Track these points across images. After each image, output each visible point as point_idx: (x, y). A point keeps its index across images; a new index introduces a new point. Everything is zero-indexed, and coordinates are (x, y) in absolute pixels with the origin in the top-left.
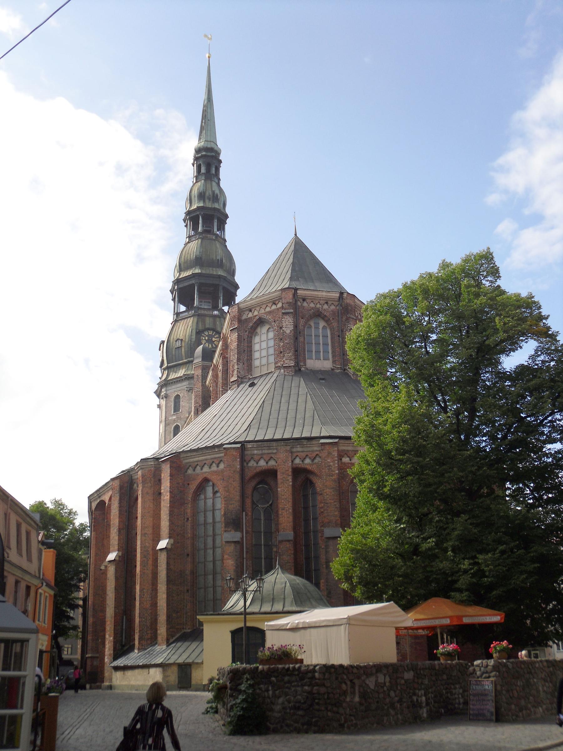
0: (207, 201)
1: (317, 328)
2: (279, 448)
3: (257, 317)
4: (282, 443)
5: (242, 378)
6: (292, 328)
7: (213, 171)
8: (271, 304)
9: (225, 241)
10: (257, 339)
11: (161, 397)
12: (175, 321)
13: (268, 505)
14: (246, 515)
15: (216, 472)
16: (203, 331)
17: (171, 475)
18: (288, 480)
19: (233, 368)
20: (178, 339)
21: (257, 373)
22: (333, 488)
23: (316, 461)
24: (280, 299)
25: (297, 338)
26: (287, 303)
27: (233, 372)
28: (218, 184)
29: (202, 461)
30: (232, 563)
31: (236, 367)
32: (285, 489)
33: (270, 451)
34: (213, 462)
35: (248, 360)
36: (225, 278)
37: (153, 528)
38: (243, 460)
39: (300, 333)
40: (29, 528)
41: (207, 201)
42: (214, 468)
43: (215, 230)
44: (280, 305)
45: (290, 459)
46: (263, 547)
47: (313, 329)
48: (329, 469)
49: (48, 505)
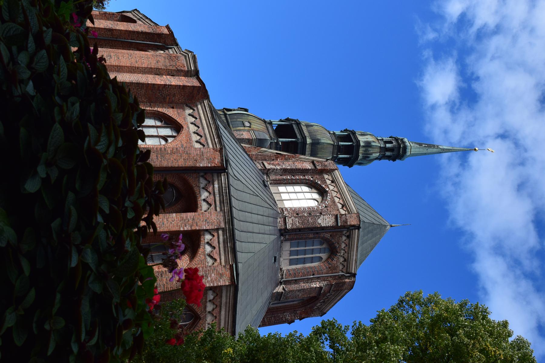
1: (320, 251)
7: (388, 154)
10: (305, 189)
15: (190, 139)
17: (184, 87)
18: (186, 226)
21: (273, 189)
23: (209, 260)
24: (349, 212)
25: (312, 230)
26: (347, 219)
27: (273, 164)
31: (279, 168)
34: (201, 136)
39: (317, 233)
41: (364, 149)
42: (195, 138)
43: (340, 156)
44: (343, 212)
45: (211, 227)
47: (319, 247)
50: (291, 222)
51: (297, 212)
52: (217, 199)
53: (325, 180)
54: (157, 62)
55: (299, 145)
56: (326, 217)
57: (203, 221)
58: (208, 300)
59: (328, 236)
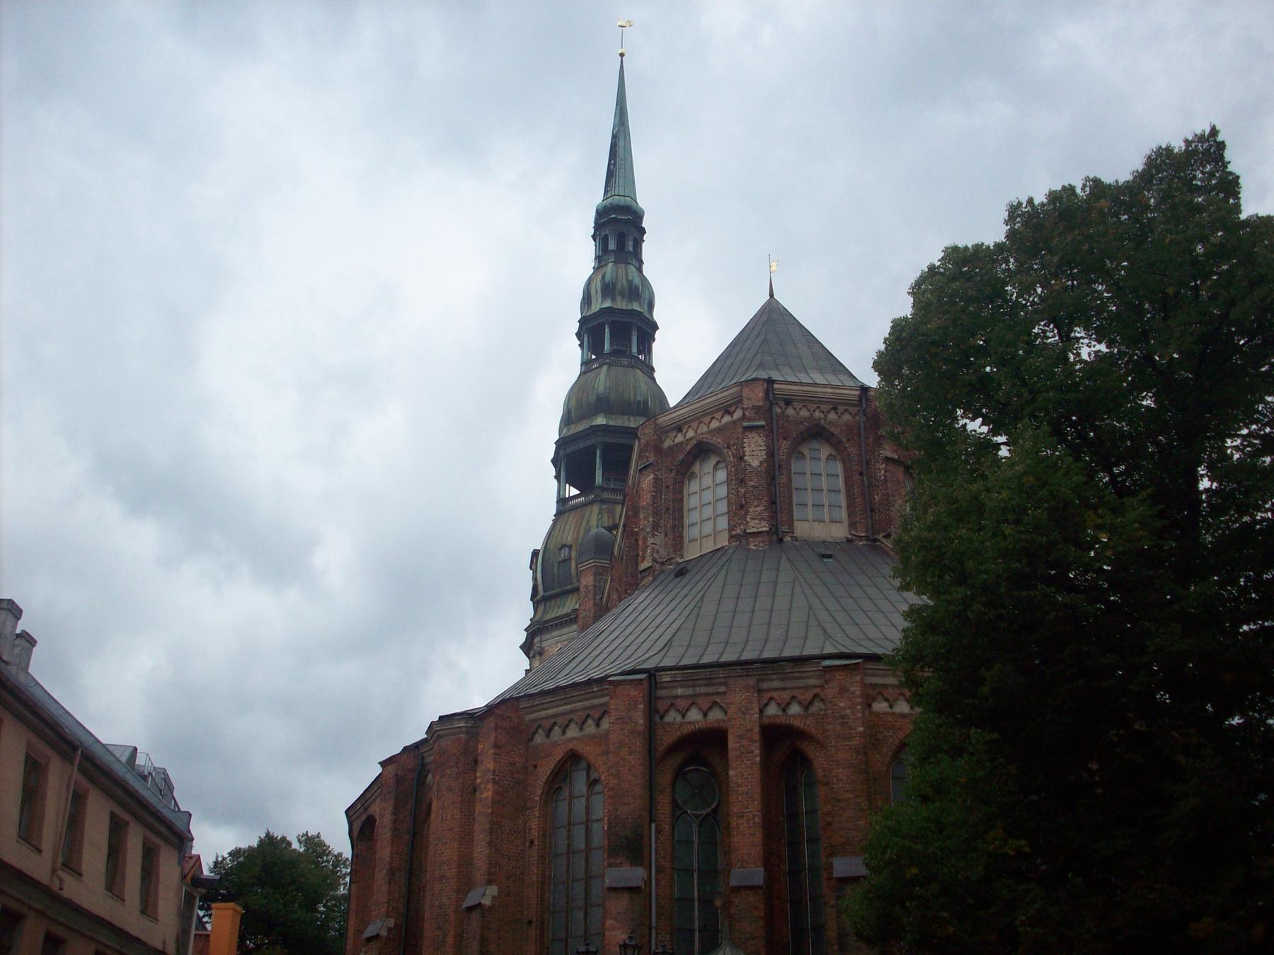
3: (694, 442)
5: (662, 563)
8: (720, 414)
9: (653, 370)
10: (694, 486)
12: (559, 514)
13: (709, 810)
14: (658, 832)
15: (593, 737)
18: (752, 752)
19: (644, 543)
20: (564, 546)
21: (692, 552)
24: (739, 401)
25: (773, 478)
26: (753, 408)
28: (640, 270)
29: (564, 714)
32: (744, 771)
33: (711, 690)
34: (588, 716)
35: (674, 527)
37: (460, 865)
38: (653, 712)
40: (156, 840)
41: (618, 298)
42: (590, 728)
43: (634, 350)
44: (738, 414)
49: (293, 847)
51: (738, 508)
52: (703, 690)
56: (747, 450)
58: (888, 710)
59: (785, 445)
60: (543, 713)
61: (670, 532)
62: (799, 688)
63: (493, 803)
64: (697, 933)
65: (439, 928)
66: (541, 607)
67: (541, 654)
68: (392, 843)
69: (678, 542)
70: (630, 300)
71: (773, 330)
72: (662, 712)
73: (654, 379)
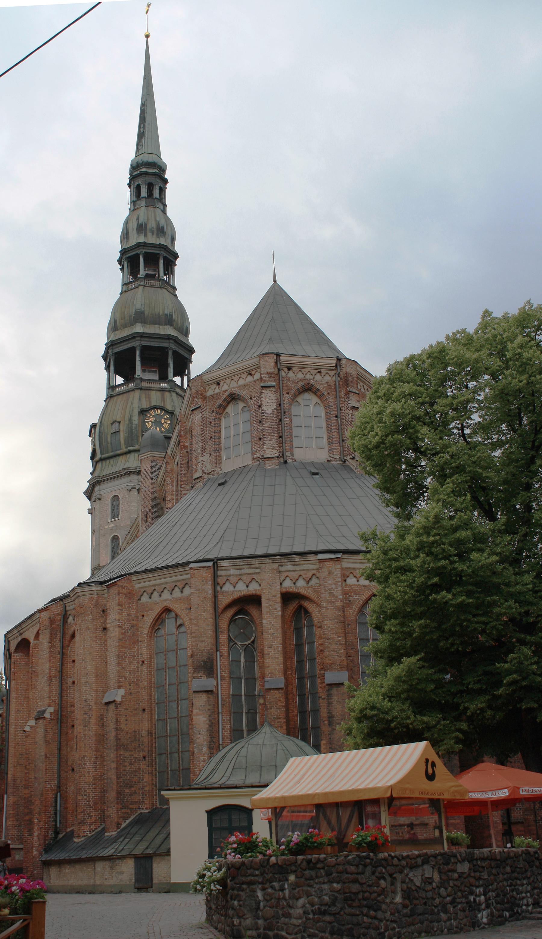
0: (149, 235)
2: (263, 566)
3: (227, 393)
4: (267, 560)
5: (208, 474)
6: (274, 406)
9: (175, 288)
11: (93, 499)
12: (109, 398)
13: (249, 642)
14: (221, 656)
16: (148, 410)
18: (276, 609)
20: (115, 422)
22: (336, 619)
23: (312, 583)
25: (281, 420)
27: (196, 465)
28: (164, 212)
29: (160, 584)
30: (205, 719)
32: (271, 620)
33: (251, 571)
34: (176, 586)
36: (176, 340)
41: (149, 235)
42: (177, 593)
44: (257, 376)
46: (243, 697)
48: (330, 593)
50: (271, 450)
53: (216, 394)
54: (89, 629)
55: (146, 343)
57: (271, 589)
58: (357, 583)
59: (287, 397)
60: (147, 584)
61: (213, 453)
62: (304, 570)
63: (119, 639)
64: (244, 714)
65: (86, 714)
66: (99, 466)
67: (100, 499)
68: (50, 660)
69: (218, 461)
70: (158, 236)
71: (276, 307)
72: (221, 585)
73: (176, 296)
